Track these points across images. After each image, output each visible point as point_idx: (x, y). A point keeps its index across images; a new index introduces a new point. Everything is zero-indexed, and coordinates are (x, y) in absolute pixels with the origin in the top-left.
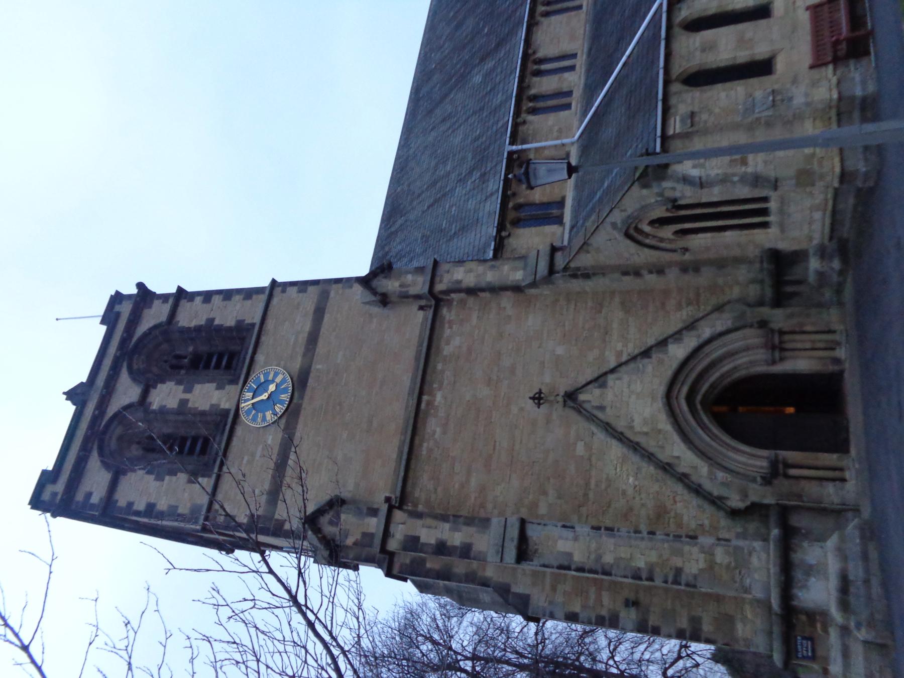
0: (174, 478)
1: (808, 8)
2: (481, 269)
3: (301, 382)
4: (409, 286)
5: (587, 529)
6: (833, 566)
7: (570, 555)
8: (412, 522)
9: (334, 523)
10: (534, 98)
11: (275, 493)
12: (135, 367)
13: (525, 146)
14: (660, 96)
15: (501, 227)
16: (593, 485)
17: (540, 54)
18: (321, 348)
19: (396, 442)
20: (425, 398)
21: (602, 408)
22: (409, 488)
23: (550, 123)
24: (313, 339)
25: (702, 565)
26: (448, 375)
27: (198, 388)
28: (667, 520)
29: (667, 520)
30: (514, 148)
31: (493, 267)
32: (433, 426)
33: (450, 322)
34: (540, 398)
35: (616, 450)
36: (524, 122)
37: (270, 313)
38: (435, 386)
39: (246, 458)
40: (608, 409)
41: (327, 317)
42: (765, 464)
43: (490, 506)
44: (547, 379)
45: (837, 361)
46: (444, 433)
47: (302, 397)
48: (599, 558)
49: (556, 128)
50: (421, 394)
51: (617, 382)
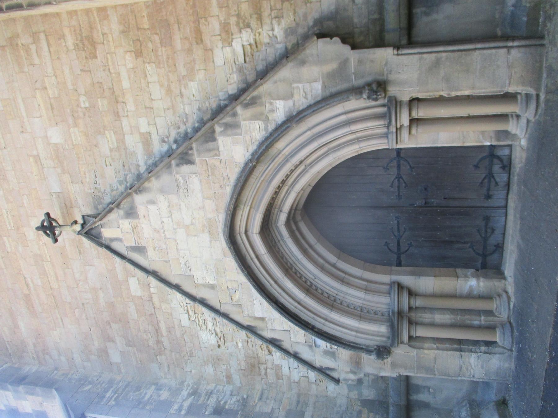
21: (140, 249)
28: (263, 371)
29: (263, 371)
40: (151, 252)
42: (383, 329)
43: (54, 353)
45: (506, 134)
51: (151, 207)
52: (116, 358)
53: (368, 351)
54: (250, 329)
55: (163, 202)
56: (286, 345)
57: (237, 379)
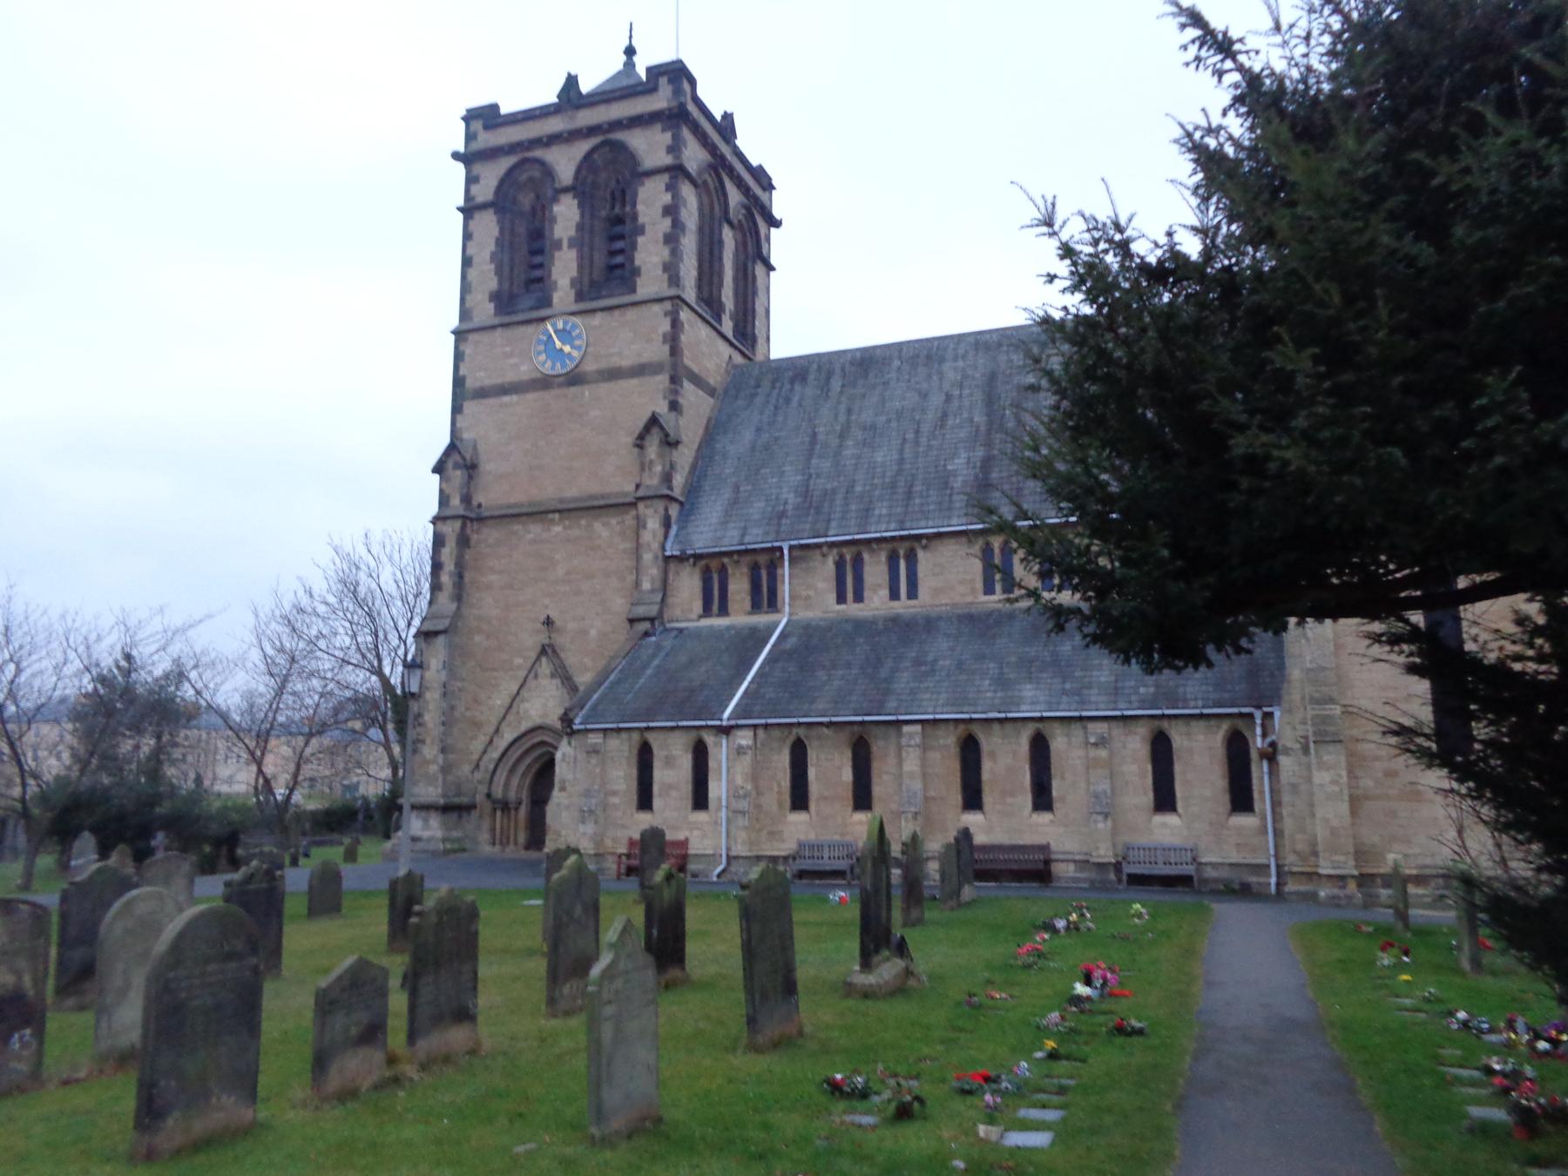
1: (687, 839)
2: (656, 546)
3: (574, 379)
4: (650, 469)
6: (426, 834)
7: (429, 669)
9: (457, 466)
10: (858, 562)
11: (482, 393)
13: (787, 564)
14: (651, 724)
15: (698, 557)
16: (495, 674)
17: (921, 554)
18: (604, 388)
20: (557, 516)
21: (536, 676)
22: (491, 522)
24: (613, 374)
25: (428, 757)
26: (575, 532)
30: (786, 552)
31: (656, 558)
32: (535, 529)
33: (623, 522)
35: (515, 688)
36: (824, 556)
37: (644, 308)
38: (567, 523)
41: (634, 382)
44: (571, 626)
46: (534, 541)
47: (560, 386)
48: (427, 689)
49: (811, 593)
50: (559, 511)
52: (477, 638)
53: (489, 788)
54: (497, 731)
56: (490, 749)
57: (468, 714)
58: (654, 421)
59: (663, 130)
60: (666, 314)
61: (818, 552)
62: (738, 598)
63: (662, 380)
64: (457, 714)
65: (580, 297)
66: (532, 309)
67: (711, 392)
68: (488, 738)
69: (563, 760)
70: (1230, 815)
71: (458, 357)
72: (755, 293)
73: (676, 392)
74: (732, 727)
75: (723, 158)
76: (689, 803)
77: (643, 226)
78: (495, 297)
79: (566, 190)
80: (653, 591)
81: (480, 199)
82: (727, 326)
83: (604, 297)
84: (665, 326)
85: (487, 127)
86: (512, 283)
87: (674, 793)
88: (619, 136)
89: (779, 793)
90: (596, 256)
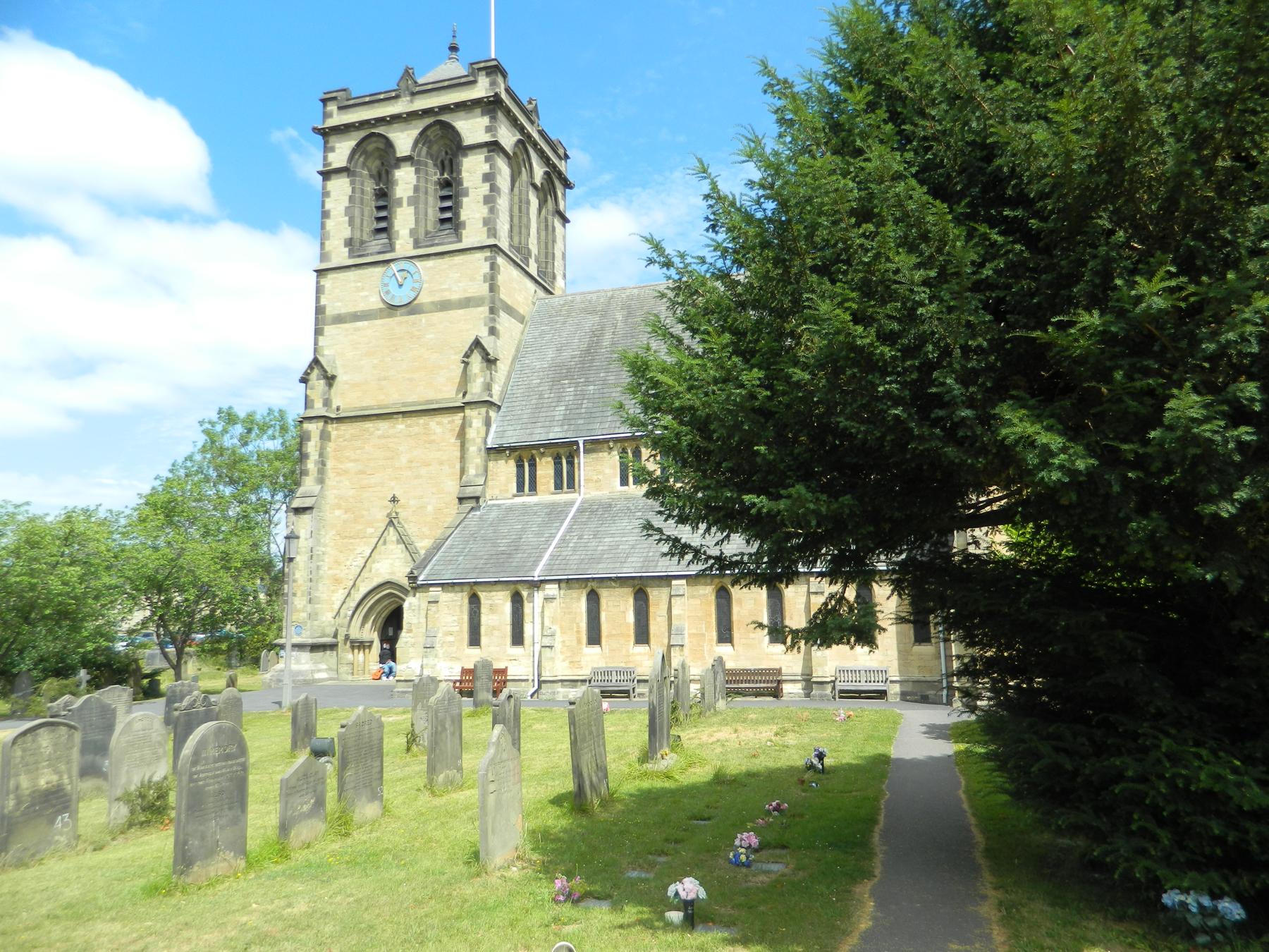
0: (347, 225)
2: (479, 441)
5: (311, 545)
8: (318, 432)
11: (339, 319)
12: (429, 133)
15: (513, 449)
19: (373, 403)
21: (385, 543)
23: (607, 471)
24: (444, 306)
26: (416, 429)
27: (411, 210)
30: (581, 445)
31: (480, 450)
32: (383, 425)
33: (453, 421)
34: (394, 501)
39: (359, 284)
44: (412, 502)
46: (379, 437)
49: (600, 477)
54: (354, 584)
55: (402, 556)
58: (477, 344)
59: (483, 114)
60: (486, 259)
61: (606, 445)
62: (544, 481)
63: (484, 310)
64: (321, 572)
65: (417, 244)
66: (379, 253)
67: (521, 319)
68: (347, 591)
69: (409, 609)
70: (914, 645)
71: (319, 290)
72: (554, 241)
73: (494, 320)
74: (542, 581)
75: (529, 136)
76: (509, 640)
77: (467, 189)
78: (349, 243)
79: (408, 159)
80: (477, 476)
81: (336, 165)
82: (533, 268)
83: (437, 245)
84: (486, 268)
85: (340, 108)
86: (362, 231)
87: (496, 633)
88: (445, 118)
89: (578, 632)
90: (430, 211)
